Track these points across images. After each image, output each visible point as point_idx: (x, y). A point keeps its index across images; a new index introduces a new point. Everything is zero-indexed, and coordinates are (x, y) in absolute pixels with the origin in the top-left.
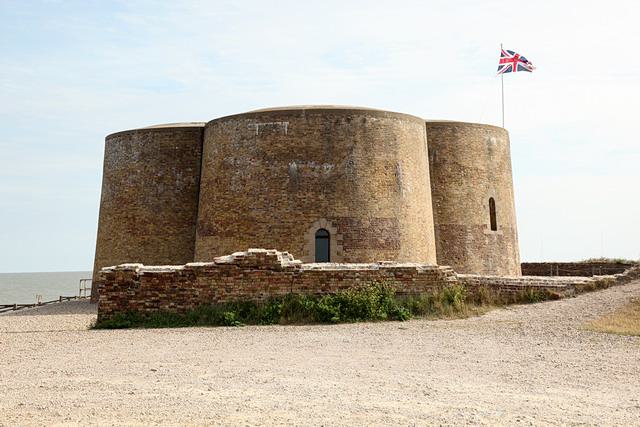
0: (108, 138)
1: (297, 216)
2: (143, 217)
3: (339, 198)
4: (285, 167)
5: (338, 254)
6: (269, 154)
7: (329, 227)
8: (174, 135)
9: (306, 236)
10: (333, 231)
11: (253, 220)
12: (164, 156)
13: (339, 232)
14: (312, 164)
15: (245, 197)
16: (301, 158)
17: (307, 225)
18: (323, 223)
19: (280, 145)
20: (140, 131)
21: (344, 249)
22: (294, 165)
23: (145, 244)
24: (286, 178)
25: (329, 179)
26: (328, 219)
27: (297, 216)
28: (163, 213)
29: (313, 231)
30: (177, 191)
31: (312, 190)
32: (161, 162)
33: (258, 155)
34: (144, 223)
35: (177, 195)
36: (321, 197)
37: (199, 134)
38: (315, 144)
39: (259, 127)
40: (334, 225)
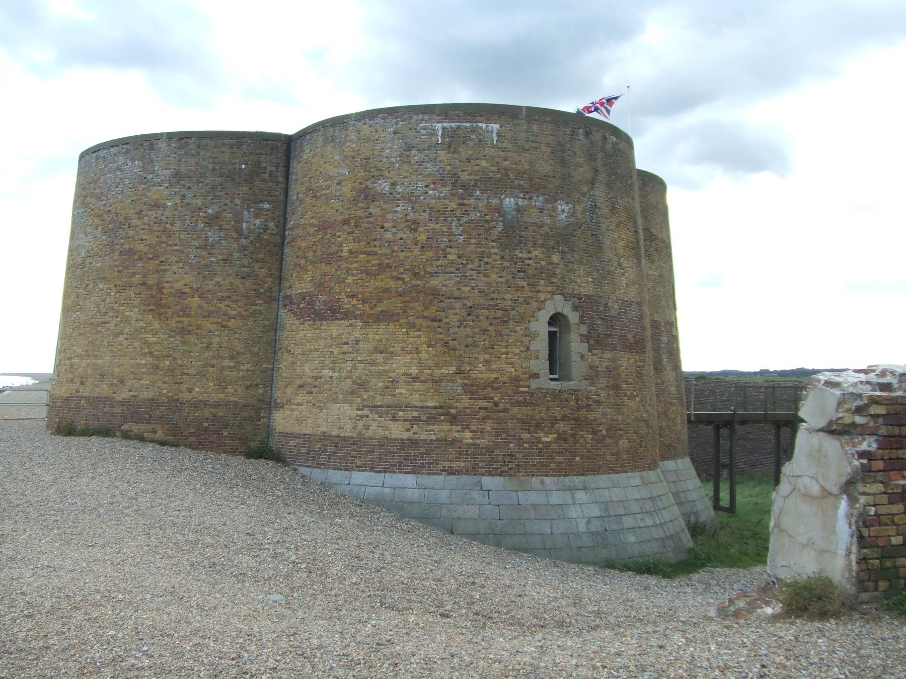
0: (82, 156)
1: (519, 288)
2: (178, 286)
3: (580, 262)
4: (495, 202)
5: (582, 357)
6: (464, 177)
7: (567, 311)
8: (241, 144)
9: (534, 326)
10: (573, 317)
11: (436, 293)
12: (219, 180)
13: (582, 322)
14: (539, 201)
15: (417, 251)
16: (521, 188)
17: (534, 305)
18: (558, 304)
19: (484, 163)
20: (171, 136)
21: (590, 351)
22: (509, 202)
23: (183, 331)
24: (497, 221)
25: (566, 228)
26: (567, 297)
27: (519, 288)
28: (217, 279)
29: (544, 316)
30: (244, 242)
31: (542, 246)
32: (214, 188)
33: (440, 180)
34: (181, 294)
35: (245, 248)
36: (555, 258)
37: (282, 149)
38: (544, 167)
39: (444, 129)
40: (575, 308)
